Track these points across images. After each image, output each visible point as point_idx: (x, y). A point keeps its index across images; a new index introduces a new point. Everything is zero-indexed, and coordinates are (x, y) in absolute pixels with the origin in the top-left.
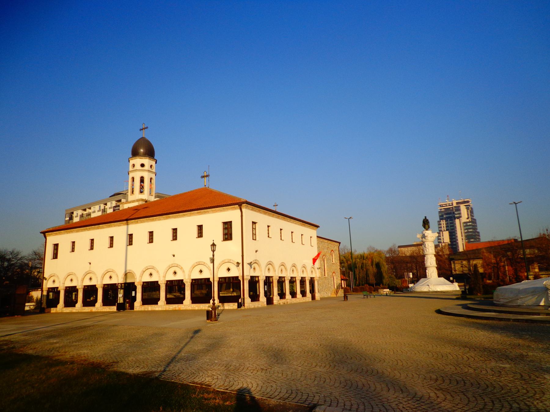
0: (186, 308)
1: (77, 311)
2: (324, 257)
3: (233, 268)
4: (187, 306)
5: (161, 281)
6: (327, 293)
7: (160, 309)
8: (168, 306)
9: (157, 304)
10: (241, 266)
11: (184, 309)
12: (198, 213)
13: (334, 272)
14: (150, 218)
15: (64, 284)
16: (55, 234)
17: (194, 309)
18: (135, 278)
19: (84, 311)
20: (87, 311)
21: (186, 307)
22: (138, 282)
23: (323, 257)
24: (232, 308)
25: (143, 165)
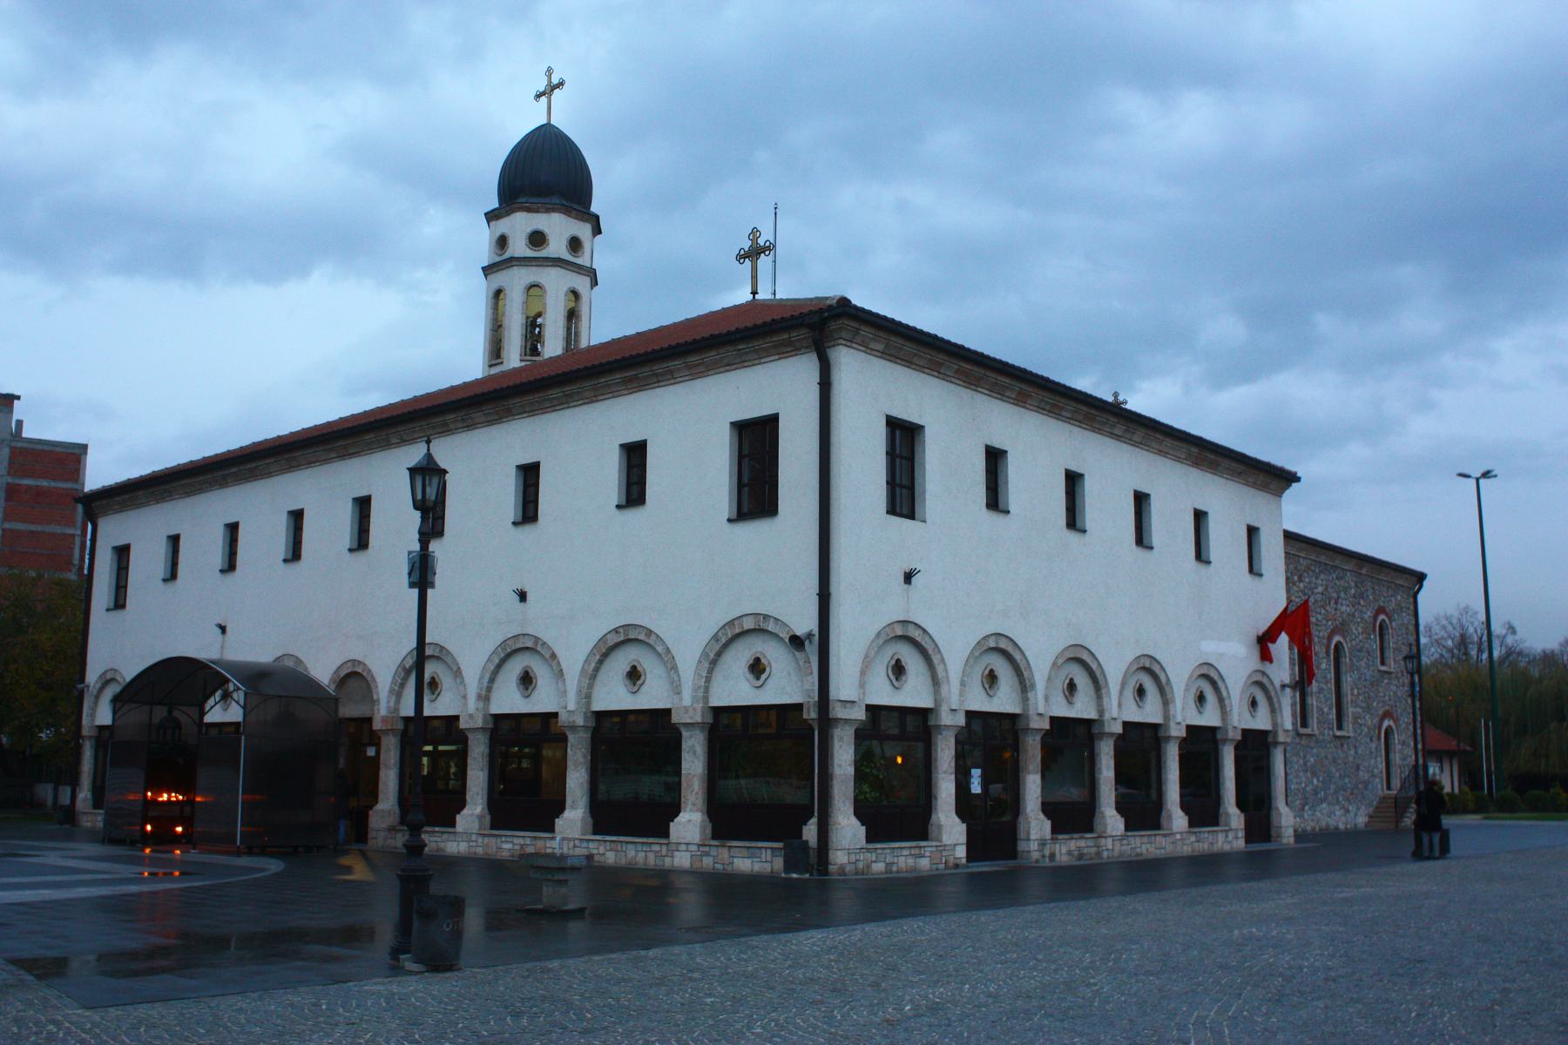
2: (1337, 638)
3: (777, 657)
4: (571, 844)
6: (1347, 811)
9: (453, 824)
10: (812, 650)
13: (1387, 715)
18: (375, 697)
22: (385, 720)
23: (1330, 638)
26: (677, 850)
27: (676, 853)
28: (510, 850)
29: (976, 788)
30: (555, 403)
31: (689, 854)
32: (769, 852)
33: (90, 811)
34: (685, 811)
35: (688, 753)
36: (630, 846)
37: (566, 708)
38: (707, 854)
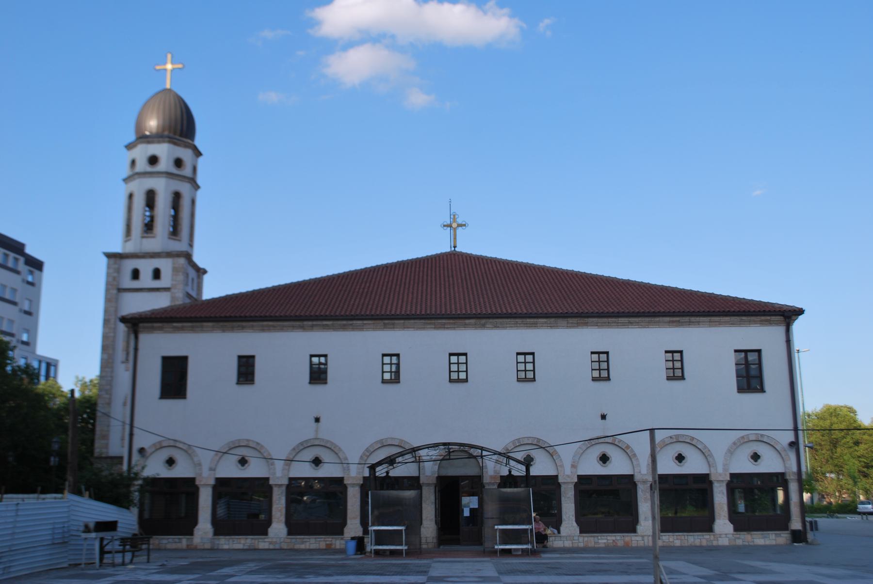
0: (646, 544)
1: (277, 547)
5: (568, 476)
7: (568, 544)
8: (592, 539)
11: (641, 544)
14: (528, 320)
15: (214, 470)
17: (672, 544)
19: (303, 547)
20: (313, 546)
21: (646, 541)
22: (491, 477)
24: (774, 543)
25: (178, 163)
26: (720, 537)
27: (719, 539)
28: (605, 543)
29: (741, 508)
30: (619, 324)
31: (727, 539)
32: (774, 535)
33: (370, 536)
35: (719, 493)
36: (690, 537)
37: (640, 472)
38: (739, 538)
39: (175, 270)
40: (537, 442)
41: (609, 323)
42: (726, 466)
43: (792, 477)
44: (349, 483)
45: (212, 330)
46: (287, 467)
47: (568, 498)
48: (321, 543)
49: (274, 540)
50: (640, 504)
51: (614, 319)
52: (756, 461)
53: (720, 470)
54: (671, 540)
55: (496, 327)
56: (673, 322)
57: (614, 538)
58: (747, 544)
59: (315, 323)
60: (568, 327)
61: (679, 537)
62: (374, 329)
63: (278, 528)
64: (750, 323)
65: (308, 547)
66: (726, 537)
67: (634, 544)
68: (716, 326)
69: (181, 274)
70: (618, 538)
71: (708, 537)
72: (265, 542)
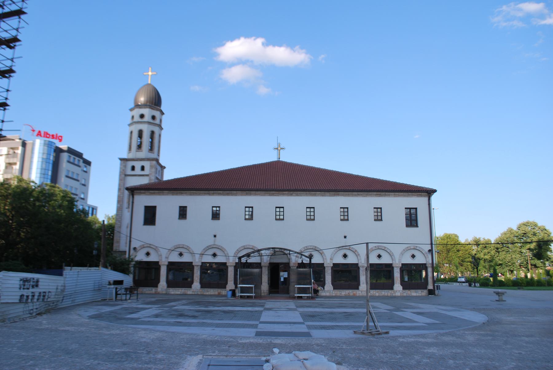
0: (363, 295)
1: (196, 293)
7: (328, 294)
8: (339, 292)
11: (361, 294)
12: (376, 194)
14: (312, 192)
15: (168, 258)
16: (150, 193)
19: (207, 293)
20: (212, 293)
22: (294, 263)
24: (420, 295)
25: (153, 118)
27: (396, 293)
28: (344, 294)
32: (420, 292)
33: (238, 289)
34: (396, 284)
36: (383, 292)
37: (361, 262)
38: (405, 293)
39: (151, 167)
40: (315, 248)
41: (349, 194)
42: (400, 260)
43: (429, 266)
44: (229, 265)
45: (167, 194)
46: (201, 257)
47: (329, 273)
48: (216, 292)
49: (194, 290)
50: (361, 276)
51: (351, 193)
52: (413, 258)
53: (397, 262)
54: (374, 293)
55: (297, 195)
56: (378, 194)
57: (349, 292)
58: (408, 295)
59: (215, 192)
60: (330, 196)
61: (378, 292)
62: (242, 195)
63: (196, 285)
64: (413, 195)
65: (210, 294)
66: (399, 292)
67: (358, 295)
68: (397, 197)
69: (154, 168)
70: (351, 292)
71: (391, 292)
72: (190, 291)
